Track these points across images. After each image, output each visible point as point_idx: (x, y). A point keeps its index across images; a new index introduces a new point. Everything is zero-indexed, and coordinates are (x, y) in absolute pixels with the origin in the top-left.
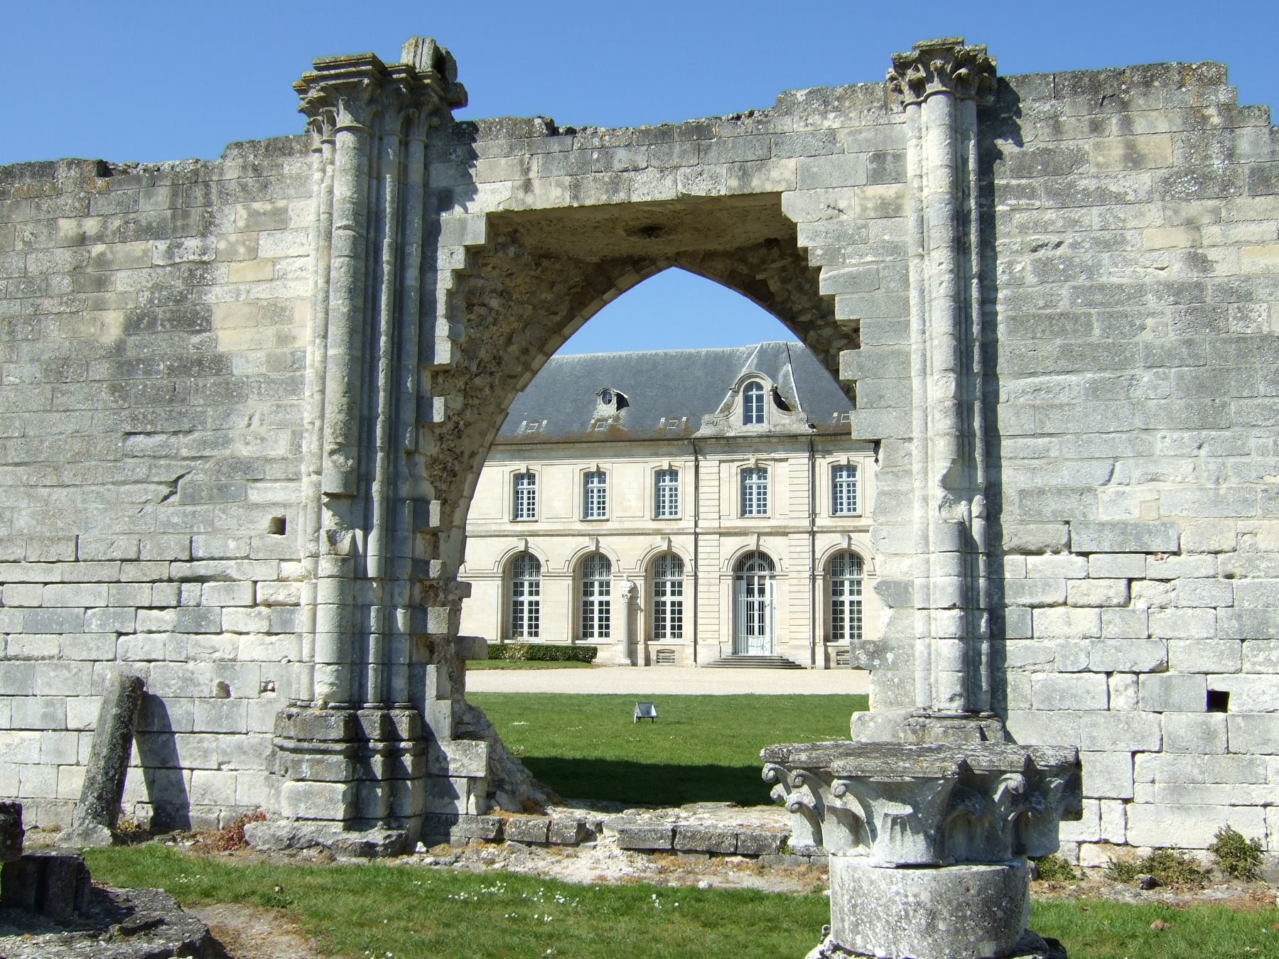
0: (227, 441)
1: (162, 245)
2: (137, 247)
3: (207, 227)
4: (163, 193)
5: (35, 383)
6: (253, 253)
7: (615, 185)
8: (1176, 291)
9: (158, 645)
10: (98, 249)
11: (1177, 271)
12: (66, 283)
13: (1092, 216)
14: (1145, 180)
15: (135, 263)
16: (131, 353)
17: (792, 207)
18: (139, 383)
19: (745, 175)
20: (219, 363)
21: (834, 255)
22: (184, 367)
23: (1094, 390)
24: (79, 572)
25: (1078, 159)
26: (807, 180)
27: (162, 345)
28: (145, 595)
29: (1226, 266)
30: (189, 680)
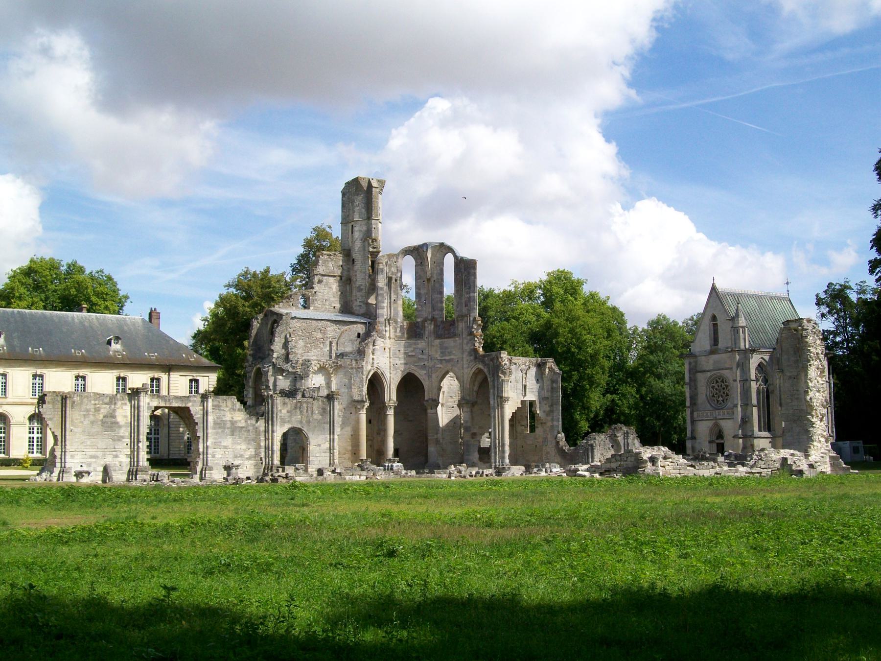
0: (119, 433)
1: (108, 406)
2: (104, 406)
3: (115, 404)
4: (108, 399)
5: (88, 424)
6: (122, 408)
7: (170, 404)
8: (230, 421)
9: (111, 460)
10: (98, 406)
11: (231, 419)
12: (93, 410)
13: (222, 412)
14: (228, 409)
15: (105, 408)
16: (104, 421)
17: (191, 408)
18: (106, 425)
19: (186, 404)
20: (118, 423)
21: (195, 415)
22: (112, 423)
23: (222, 431)
24: (97, 450)
25: (221, 406)
26: (193, 405)
27: (109, 420)
28: (108, 453)
29: (235, 419)
30: (115, 464)
